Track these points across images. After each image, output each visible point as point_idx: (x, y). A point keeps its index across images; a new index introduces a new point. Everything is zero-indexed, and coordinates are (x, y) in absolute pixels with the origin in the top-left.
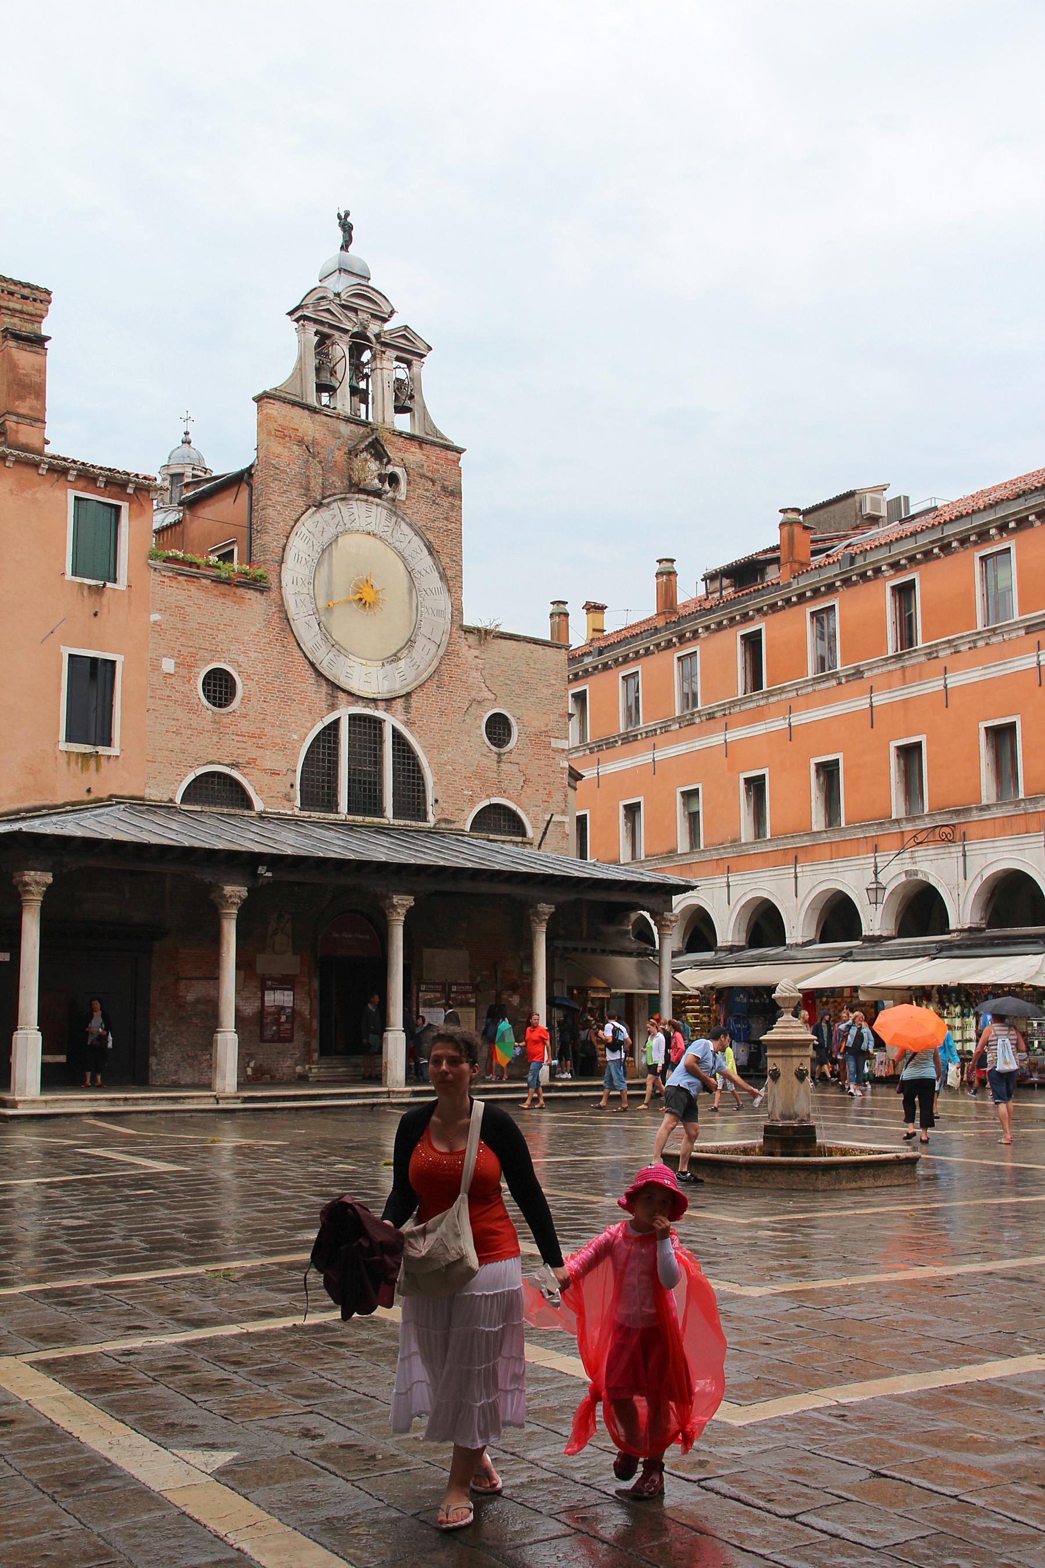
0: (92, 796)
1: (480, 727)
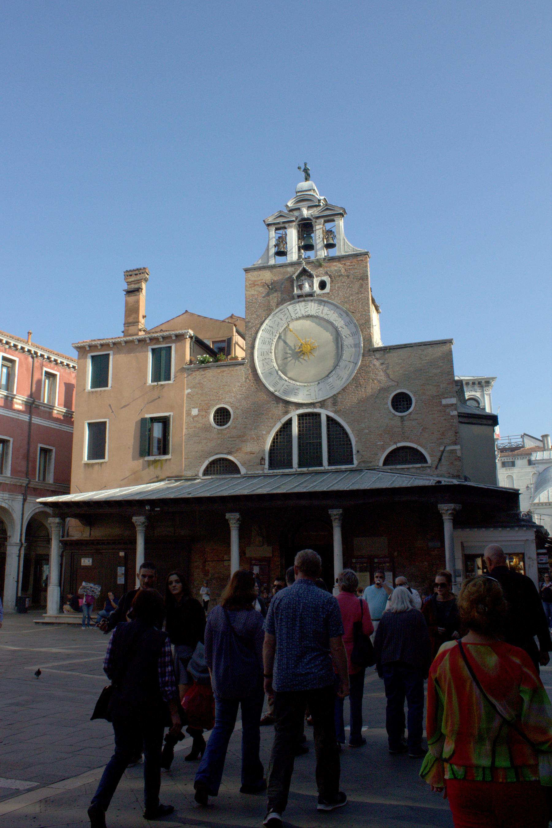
0: (160, 478)
1: (387, 403)
